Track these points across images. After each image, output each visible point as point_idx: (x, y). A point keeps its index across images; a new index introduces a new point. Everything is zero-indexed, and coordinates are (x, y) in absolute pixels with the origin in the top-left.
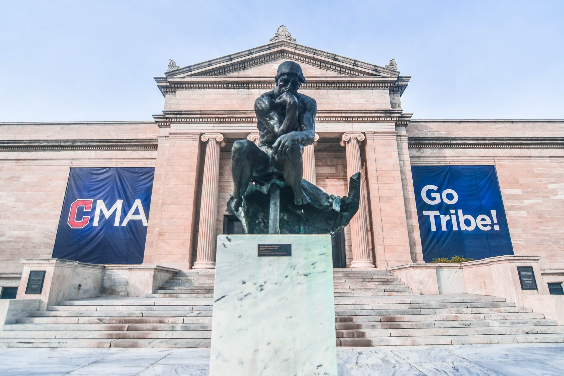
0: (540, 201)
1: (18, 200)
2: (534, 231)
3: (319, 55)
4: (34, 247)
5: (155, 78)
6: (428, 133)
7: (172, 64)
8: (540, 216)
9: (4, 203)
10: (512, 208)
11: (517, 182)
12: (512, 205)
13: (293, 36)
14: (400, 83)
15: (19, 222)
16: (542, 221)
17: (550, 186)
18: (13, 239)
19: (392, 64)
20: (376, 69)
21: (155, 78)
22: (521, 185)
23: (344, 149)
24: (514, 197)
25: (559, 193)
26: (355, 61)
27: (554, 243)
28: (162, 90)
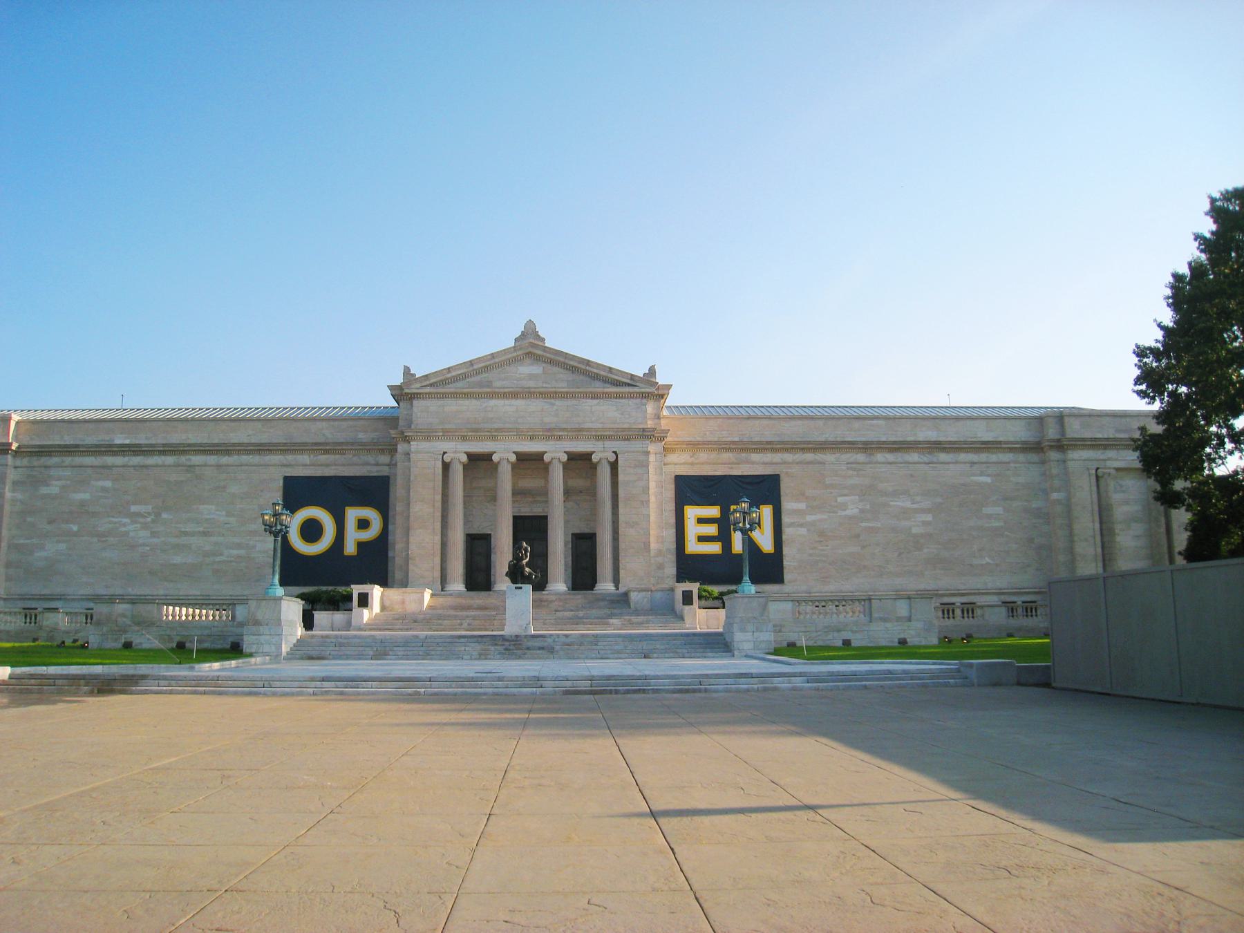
0: (825, 516)
1: (229, 514)
2: (811, 551)
3: (571, 360)
4: (259, 568)
5: (388, 386)
6: (707, 433)
7: (407, 371)
8: (822, 534)
9: (213, 519)
10: (791, 525)
11: (803, 494)
12: (792, 521)
13: (541, 334)
14: (660, 392)
15: (236, 540)
16: (822, 540)
17: (840, 499)
18: (232, 559)
19: (652, 371)
20: (632, 377)
21: (388, 386)
22: (807, 498)
23: (594, 467)
24: (796, 512)
25: (849, 507)
26: (610, 368)
27: (830, 564)
28: (396, 398)
